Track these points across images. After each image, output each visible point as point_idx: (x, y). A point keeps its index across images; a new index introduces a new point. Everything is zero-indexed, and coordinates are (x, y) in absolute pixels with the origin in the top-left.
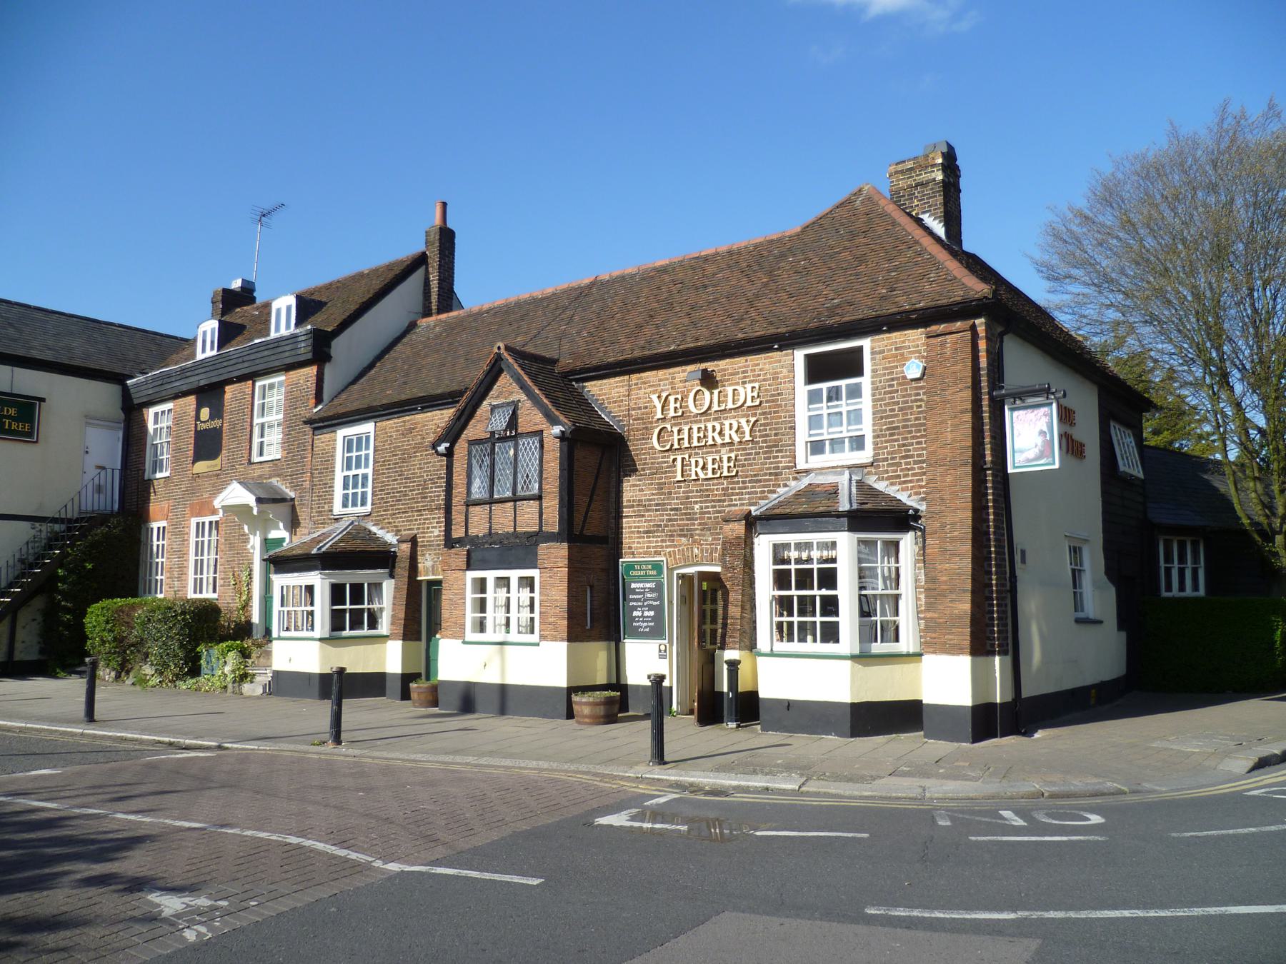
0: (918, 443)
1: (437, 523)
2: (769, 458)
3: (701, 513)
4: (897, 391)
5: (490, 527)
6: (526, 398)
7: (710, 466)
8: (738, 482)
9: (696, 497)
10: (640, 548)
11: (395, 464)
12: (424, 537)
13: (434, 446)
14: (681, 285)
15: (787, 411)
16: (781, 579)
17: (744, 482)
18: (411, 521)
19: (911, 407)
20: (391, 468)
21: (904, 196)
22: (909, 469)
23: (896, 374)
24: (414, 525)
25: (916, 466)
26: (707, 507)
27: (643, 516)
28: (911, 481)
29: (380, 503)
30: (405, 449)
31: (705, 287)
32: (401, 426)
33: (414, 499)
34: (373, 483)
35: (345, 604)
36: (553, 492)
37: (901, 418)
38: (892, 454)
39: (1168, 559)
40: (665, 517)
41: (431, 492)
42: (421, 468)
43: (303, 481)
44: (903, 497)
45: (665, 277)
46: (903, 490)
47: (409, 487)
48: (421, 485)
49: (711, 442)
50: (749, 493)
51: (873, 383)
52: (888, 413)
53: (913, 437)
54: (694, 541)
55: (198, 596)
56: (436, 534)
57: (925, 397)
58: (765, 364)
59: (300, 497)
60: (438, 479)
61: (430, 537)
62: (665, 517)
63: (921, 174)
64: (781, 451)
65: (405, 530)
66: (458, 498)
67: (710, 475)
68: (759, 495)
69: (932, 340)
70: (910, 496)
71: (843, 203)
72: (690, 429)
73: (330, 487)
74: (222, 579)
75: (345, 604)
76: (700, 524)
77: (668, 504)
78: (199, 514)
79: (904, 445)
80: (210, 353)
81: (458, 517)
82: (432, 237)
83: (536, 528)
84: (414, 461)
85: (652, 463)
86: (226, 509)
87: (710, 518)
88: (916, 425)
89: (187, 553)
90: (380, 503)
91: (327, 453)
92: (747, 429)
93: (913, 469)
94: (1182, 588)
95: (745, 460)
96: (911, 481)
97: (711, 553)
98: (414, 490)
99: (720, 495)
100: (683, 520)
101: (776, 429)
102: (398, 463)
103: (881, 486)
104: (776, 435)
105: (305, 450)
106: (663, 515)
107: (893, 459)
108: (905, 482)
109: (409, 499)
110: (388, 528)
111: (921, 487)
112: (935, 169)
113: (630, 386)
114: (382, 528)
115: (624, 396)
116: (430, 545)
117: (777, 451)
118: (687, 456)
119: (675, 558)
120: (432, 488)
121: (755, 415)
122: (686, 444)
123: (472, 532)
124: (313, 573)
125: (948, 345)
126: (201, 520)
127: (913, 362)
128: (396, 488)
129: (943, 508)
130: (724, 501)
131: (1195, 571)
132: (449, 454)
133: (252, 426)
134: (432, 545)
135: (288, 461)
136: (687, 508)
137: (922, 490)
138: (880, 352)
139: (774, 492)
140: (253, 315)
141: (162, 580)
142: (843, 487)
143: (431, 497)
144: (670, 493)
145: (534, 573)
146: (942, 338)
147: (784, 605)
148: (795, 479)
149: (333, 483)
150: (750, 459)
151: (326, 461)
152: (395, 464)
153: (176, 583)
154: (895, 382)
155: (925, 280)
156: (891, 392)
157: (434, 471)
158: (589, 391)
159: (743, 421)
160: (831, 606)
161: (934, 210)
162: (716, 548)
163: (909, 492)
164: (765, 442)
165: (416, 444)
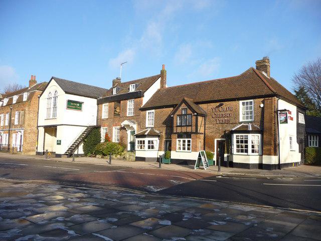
16: (238, 142)
131: (316, 142)
147: (238, 146)
160: (247, 147)
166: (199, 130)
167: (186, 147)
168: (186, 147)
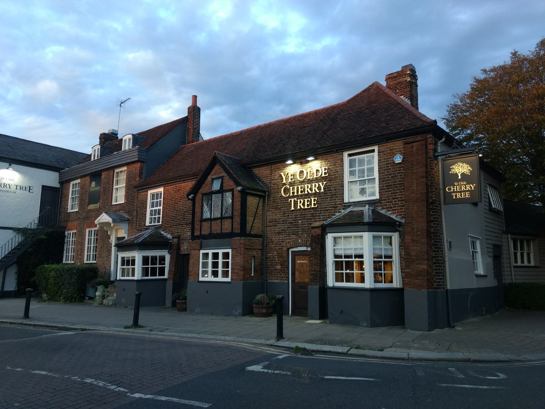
0: (400, 192)
3: (302, 224)
5: (211, 231)
6: (226, 175)
7: (306, 203)
8: (318, 211)
9: (300, 217)
10: (276, 240)
11: (172, 204)
12: (184, 236)
14: (294, 127)
15: (340, 179)
17: (321, 211)
18: (178, 229)
19: (397, 176)
20: (171, 206)
21: (393, 88)
22: (396, 204)
23: (390, 161)
24: (180, 231)
25: (399, 202)
26: (305, 222)
27: (277, 226)
28: (397, 209)
29: (165, 221)
30: (176, 198)
31: (305, 127)
33: (180, 219)
35: (149, 265)
37: (392, 181)
38: (388, 197)
39: (515, 248)
40: (286, 226)
41: (187, 217)
42: (183, 206)
43: (133, 212)
44: (393, 217)
45: (288, 124)
46: (393, 213)
47: (178, 214)
48: (183, 213)
49: (306, 193)
52: (386, 179)
53: (398, 190)
54: (299, 237)
55: (88, 262)
57: (403, 171)
58: (330, 159)
61: (186, 236)
62: (286, 226)
64: (337, 197)
65: (175, 233)
66: (197, 219)
67: (306, 207)
69: (408, 146)
72: (298, 188)
73: (144, 215)
74: (98, 255)
76: (301, 229)
78: (89, 227)
79: (394, 193)
81: (197, 227)
82: (191, 110)
83: (230, 231)
84: (180, 203)
85: (281, 203)
86: (100, 224)
87: (305, 227)
89: (84, 244)
90: (165, 221)
93: (398, 204)
94: (522, 262)
95: (321, 201)
96: (397, 209)
97: (306, 242)
98: (180, 216)
99: (310, 217)
101: (335, 187)
102: (173, 204)
103: (383, 212)
104: (335, 190)
106: (285, 225)
107: (388, 199)
108: (394, 210)
109: (178, 220)
110: (168, 232)
112: (406, 76)
113: (271, 170)
114: (166, 232)
115: (269, 174)
117: (335, 197)
118: (296, 199)
119: (290, 244)
120: (187, 215)
122: (296, 194)
123: (203, 233)
124: (134, 252)
125: (414, 147)
126: (90, 229)
127: (398, 156)
128: (172, 215)
129: (413, 221)
130: (312, 219)
132: (193, 200)
133: (112, 189)
134: (187, 239)
135: (127, 204)
136: (296, 222)
137: (402, 213)
138: (383, 152)
139: (334, 215)
141: (73, 255)
142: (366, 212)
143: (187, 218)
144: (288, 216)
145: (230, 251)
146: (412, 144)
148: (343, 209)
149: (146, 213)
150: (323, 201)
151: (143, 204)
152: (172, 204)
153: (79, 256)
154: (389, 165)
155: (403, 119)
156: (387, 170)
157: (188, 207)
158: (254, 172)
159: (321, 184)
161: (406, 94)
162: (308, 240)
163: (396, 215)
164: (330, 193)
165: (181, 196)
167: (220, 269)
168: (220, 269)
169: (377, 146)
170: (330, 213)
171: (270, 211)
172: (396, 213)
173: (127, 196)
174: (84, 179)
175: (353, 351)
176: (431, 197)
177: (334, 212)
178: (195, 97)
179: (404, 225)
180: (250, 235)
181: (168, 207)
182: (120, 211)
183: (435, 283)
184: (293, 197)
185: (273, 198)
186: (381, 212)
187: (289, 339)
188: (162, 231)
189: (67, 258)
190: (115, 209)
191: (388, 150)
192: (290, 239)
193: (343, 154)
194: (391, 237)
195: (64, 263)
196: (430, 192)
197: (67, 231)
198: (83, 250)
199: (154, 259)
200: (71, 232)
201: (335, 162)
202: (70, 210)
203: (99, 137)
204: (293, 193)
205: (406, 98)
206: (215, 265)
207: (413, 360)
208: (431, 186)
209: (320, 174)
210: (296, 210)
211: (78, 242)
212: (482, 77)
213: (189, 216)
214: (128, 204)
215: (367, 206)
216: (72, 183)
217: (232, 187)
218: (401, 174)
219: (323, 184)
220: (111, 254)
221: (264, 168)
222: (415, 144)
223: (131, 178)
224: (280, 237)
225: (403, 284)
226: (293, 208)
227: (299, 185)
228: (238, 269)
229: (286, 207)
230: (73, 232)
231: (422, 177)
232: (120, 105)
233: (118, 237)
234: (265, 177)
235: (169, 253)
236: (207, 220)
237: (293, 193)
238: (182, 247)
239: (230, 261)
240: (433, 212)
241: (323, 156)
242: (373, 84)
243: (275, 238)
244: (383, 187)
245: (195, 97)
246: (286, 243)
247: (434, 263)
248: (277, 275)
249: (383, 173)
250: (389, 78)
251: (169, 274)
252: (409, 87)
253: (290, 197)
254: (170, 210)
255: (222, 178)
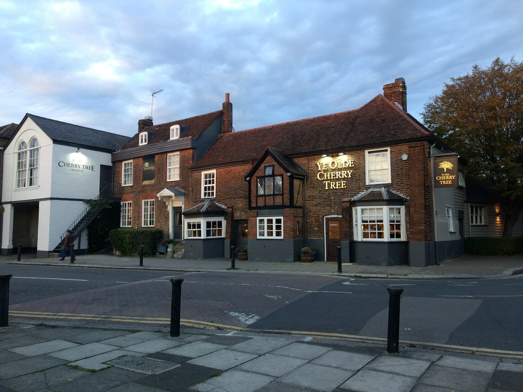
0: (406, 179)
1: (241, 202)
2: (357, 183)
3: (334, 200)
4: (399, 163)
7: (337, 185)
8: (346, 190)
9: (332, 194)
10: (314, 210)
11: (224, 183)
13: (245, 178)
15: (363, 169)
17: (348, 190)
18: (231, 201)
19: (404, 168)
20: (223, 184)
22: (403, 187)
24: (232, 202)
26: (336, 198)
27: (314, 200)
28: (404, 191)
32: (226, 171)
34: (216, 189)
35: (211, 228)
36: (288, 193)
37: (400, 172)
39: (472, 213)
41: (239, 192)
42: (234, 185)
44: (401, 195)
46: (401, 193)
48: (235, 190)
49: (337, 177)
50: (350, 194)
51: (391, 161)
52: (396, 170)
53: (404, 178)
54: (332, 208)
56: (240, 205)
57: (408, 166)
59: (188, 193)
60: (240, 188)
61: (239, 206)
62: (322, 201)
63: (395, 89)
65: (229, 204)
67: (337, 187)
68: (354, 194)
70: (403, 195)
71: (373, 101)
72: (330, 174)
75: (211, 228)
76: (334, 203)
77: (323, 197)
78: (146, 199)
79: (402, 180)
80: (144, 144)
82: (225, 105)
83: (282, 204)
84: (232, 182)
85: (317, 184)
86: (161, 197)
87: (337, 201)
88: (405, 174)
91: (197, 179)
92: (350, 174)
94: (476, 222)
95: (349, 183)
96: (404, 191)
98: (232, 191)
99: (340, 194)
100: (328, 201)
101: (359, 174)
102: (225, 183)
103: (394, 192)
104: (359, 176)
105: (189, 178)
108: (402, 191)
109: (230, 194)
111: (407, 192)
112: (399, 87)
114: (220, 204)
115: (307, 163)
116: (238, 209)
117: (359, 181)
118: (329, 182)
119: (325, 213)
120: (238, 191)
121: (351, 170)
122: (329, 178)
123: (259, 205)
124: (200, 218)
126: (146, 200)
129: (415, 199)
130: (342, 196)
131: (481, 217)
132: (249, 182)
133: (166, 169)
138: (393, 152)
139: (359, 193)
140: (156, 130)
142: (383, 192)
143: (238, 194)
144: (323, 193)
145: (282, 218)
146: (414, 148)
149: (201, 189)
151: (197, 181)
152: (224, 183)
155: (407, 129)
158: (294, 161)
159: (348, 171)
161: (399, 101)
162: (339, 210)
164: (356, 178)
166: (295, 200)
167: (274, 230)
168: (274, 230)
169: (390, 148)
170: (355, 192)
171: (309, 189)
172: (403, 193)
173: (182, 175)
174: (136, 160)
175: (389, 276)
176: (427, 183)
177: (358, 191)
178: (228, 95)
179: (408, 201)
180: (296, 207)
181: (221, 185)
182: (175, 186)
183: (429, 238)
184: (327, 180)
185: (310, 180)
186: (392, 192)
187: (346, 272)
188: (217, 203)
189: (124, 223)
190: (170, 185)
191: (397, 151)
192: (325, 209)
193: (364, 152)
194: (400, 209)
195: (121, 227)
196: (426, 180)
197: (123, 201)
198: (140, 216)
199: (214, 223)
200: (127, 202)
201: (359, 157)
202: (123, 185)
203: (138, 123)
204: (327, 177)
205: (399, 104)
206: (270, 228)
207: (426, 279)
208: (427, 176)
209: (347, 166)
210: (329, 189)
211: (134, 210)
212: (451, 83)
213: (240, 192)
214: (183, 181)
215: (383, 188)
216: (123, 163)
217: (282, 173)
218: (406, 167)
219: (350, 172)
220: (169, 220)
221: (302, 158)
222: (416, 148)
223: (185, 161)
224: (317, 208)
225: (408, 238)
226: (327, 188)
227: (332, 172)
228: (289, 231)
229: (322, 187)
230: (129, 202)
231: (421, 170)
232: (153, 95)
233: (174, 206)
234: (304, 165)
235: (225, 219)
236: (261, 196)
237: (327, 177)
238: (235, 215)
239: (282, 224)
240: (428, 193)
241: (350, 152)
242: (378, 96)
243: (313, 209)
244: (394, 175)
245: (228, 95)
246: (322, 212)
247: (428, 225)
248: (315, 234)
249: (394, 166)
250: (386, 88)
251: (226, 234)
252: (401, 96)
253: (324, 180)
254: (223, 187)
255: (273, 166)
